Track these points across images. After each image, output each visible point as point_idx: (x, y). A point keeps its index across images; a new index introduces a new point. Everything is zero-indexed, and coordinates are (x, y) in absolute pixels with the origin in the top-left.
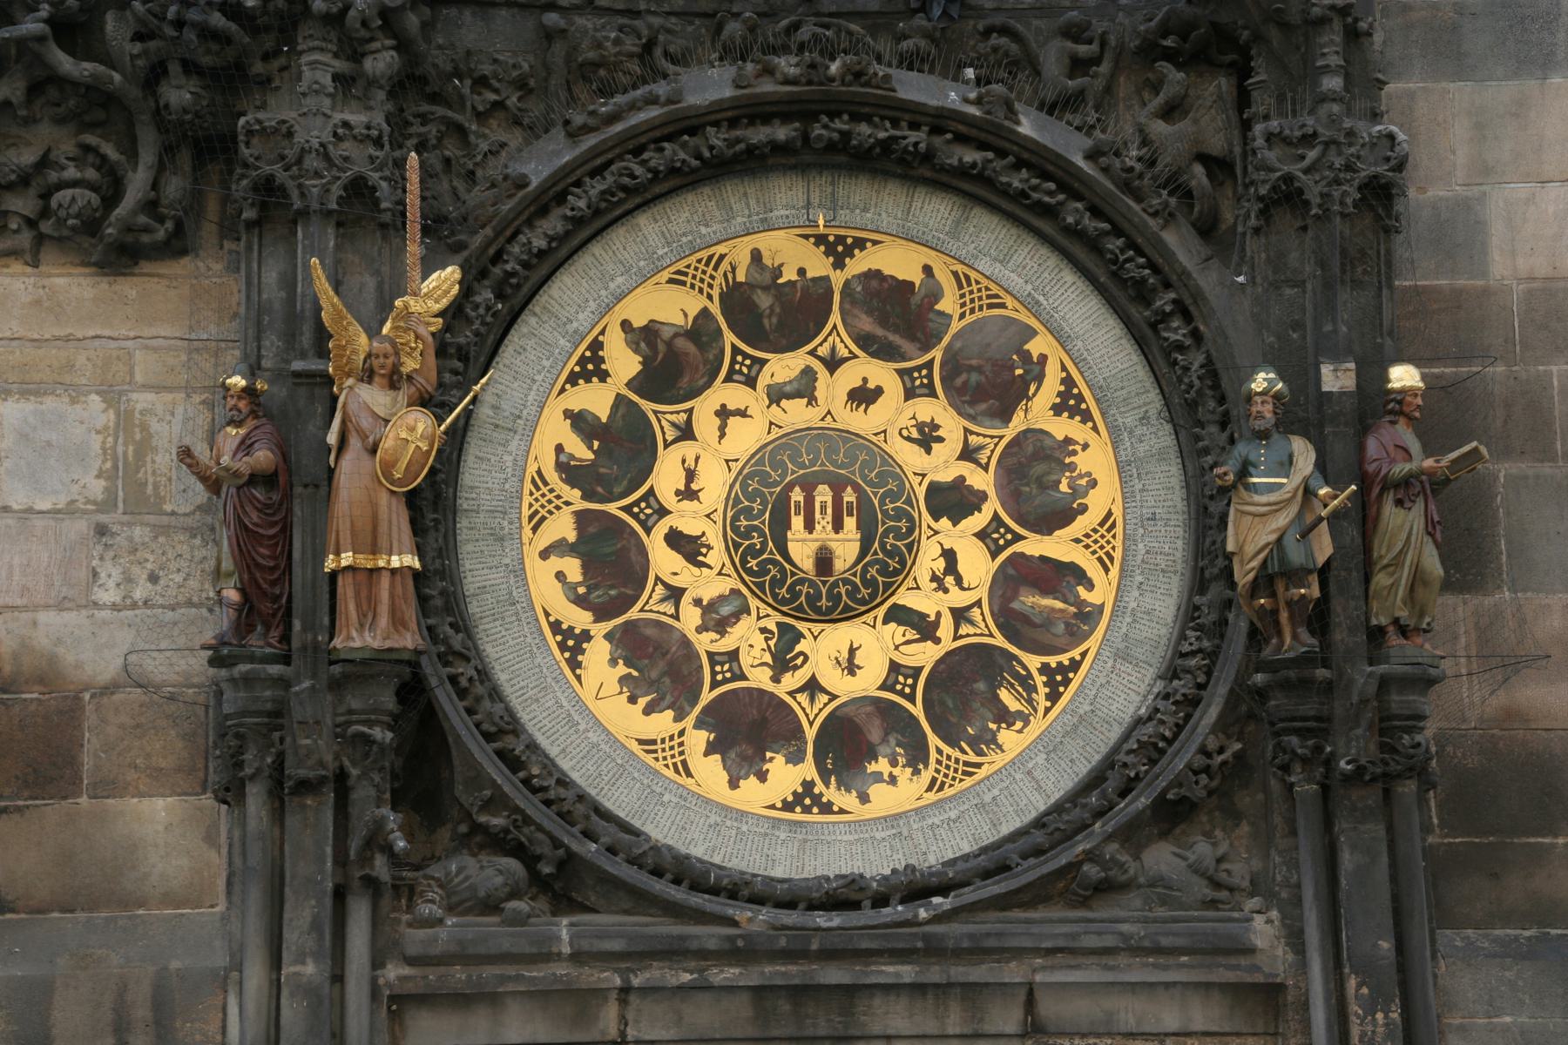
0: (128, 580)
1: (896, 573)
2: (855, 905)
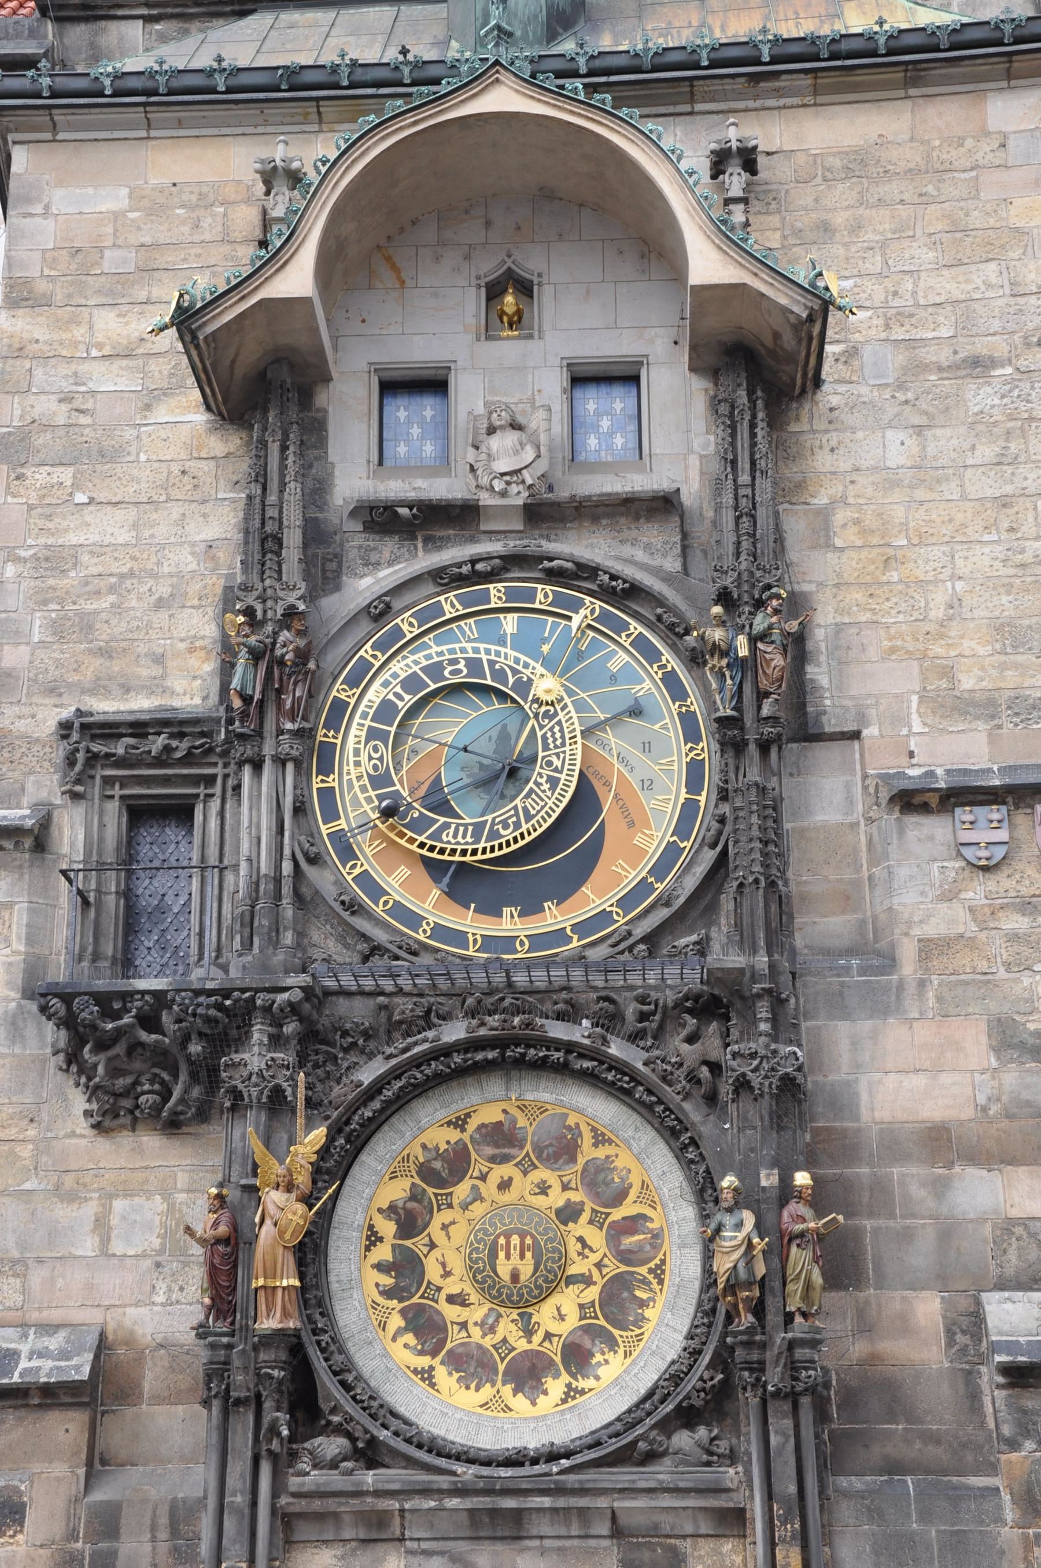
0: (170, 1289)
1: (552, 1281)
2: (521, 1464)
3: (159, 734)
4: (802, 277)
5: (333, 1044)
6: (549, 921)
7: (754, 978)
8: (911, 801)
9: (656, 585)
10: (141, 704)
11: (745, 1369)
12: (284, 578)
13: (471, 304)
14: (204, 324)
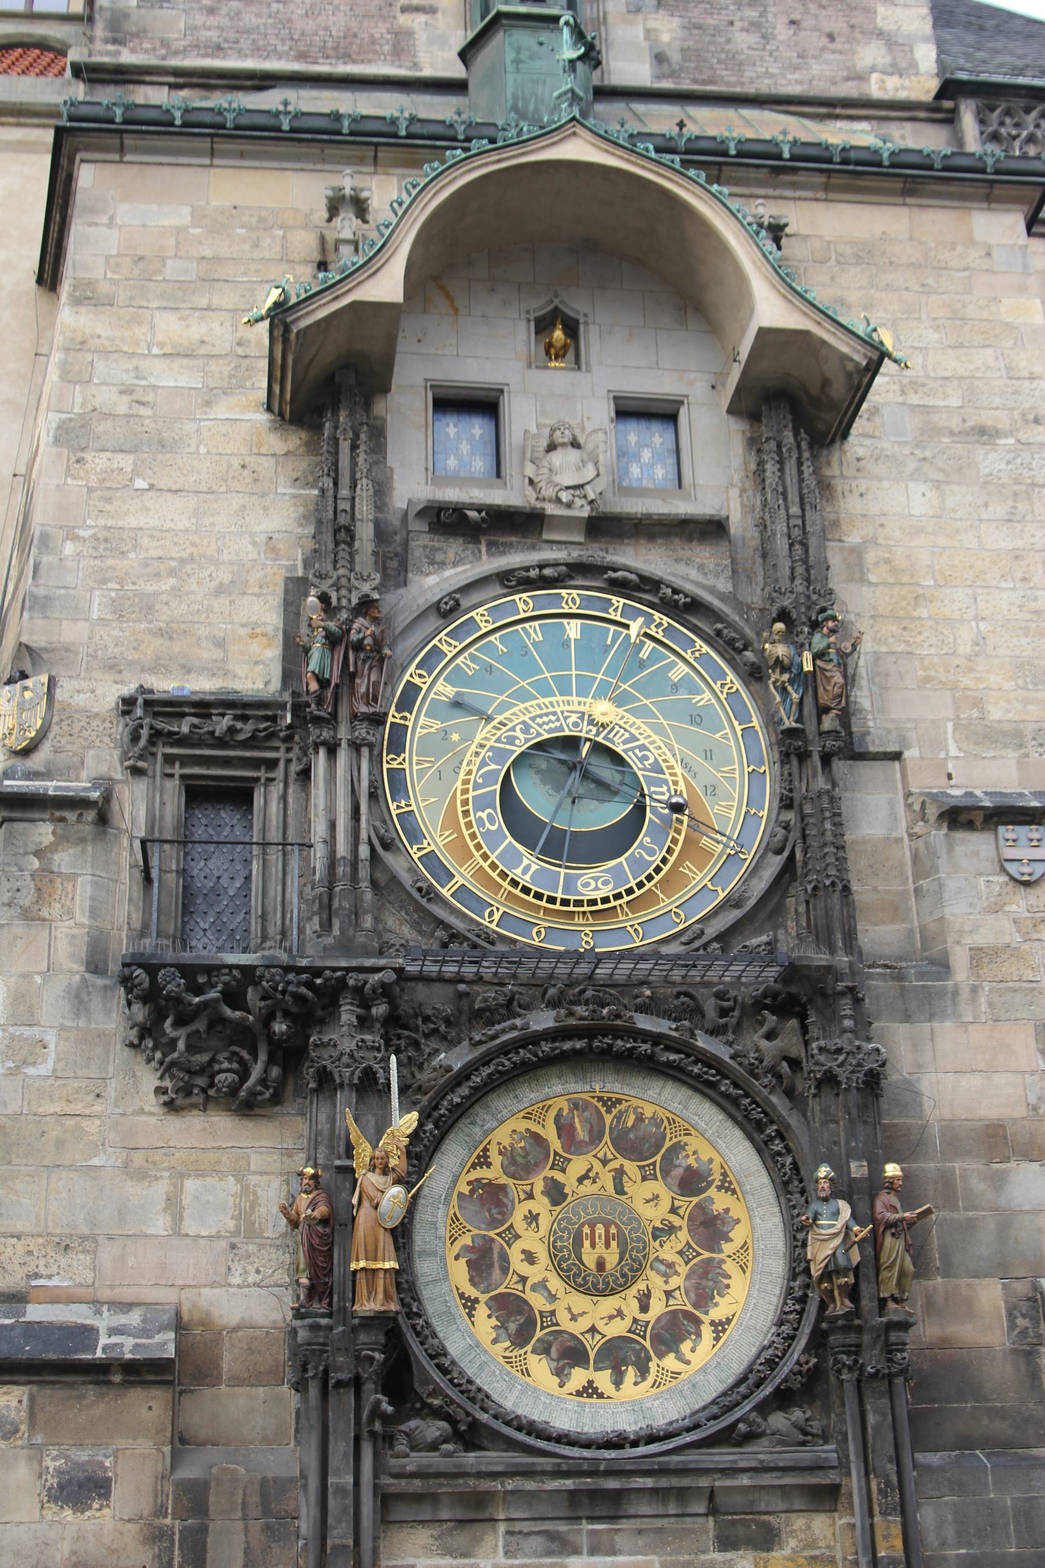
1: (637, 1270)
3: (223, 715)
4: (861, 330)
5: (416, 1029)
6: (621, 918)
7: (839, 977)
8: (959, 817)
9: (716, 603)
10: (201, 685)
12: (357, 568)
13: (521, 335)
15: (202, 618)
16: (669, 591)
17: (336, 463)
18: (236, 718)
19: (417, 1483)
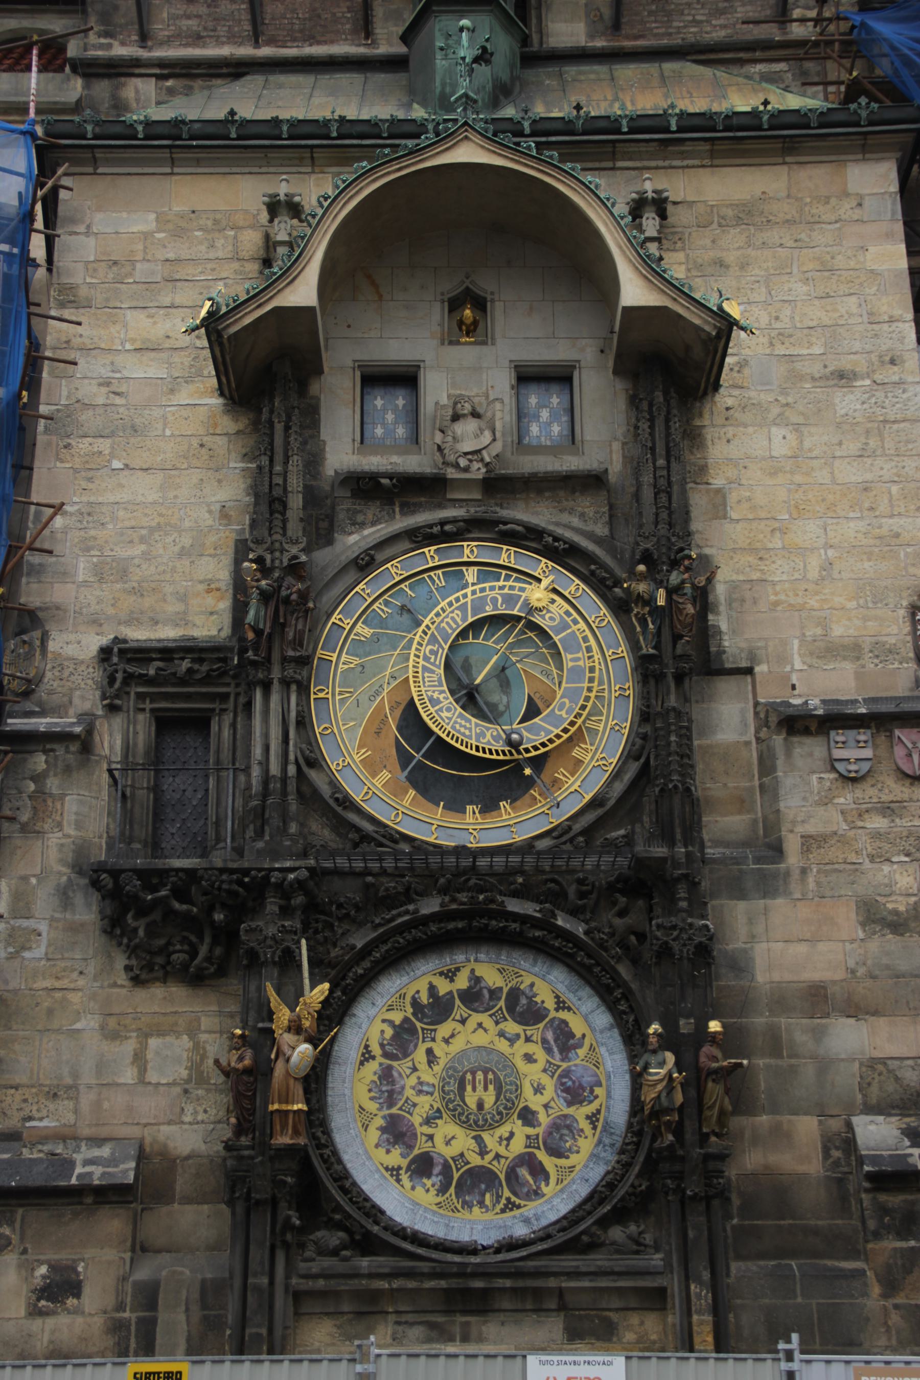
0: (196, 1112)
3: (183, 659)
4: (712, 305)
5: (329, 914)
6: (505, 817)
7: (676, 865)
8: (796, 724)
10: (168, 633)
11: (666, 1178)
12: (289, 533)
14: (228, 326)
15: (168, 577)
16: (550, 539)
17: (271, 444)
18: (193, 660)
19: (321, 1283)
